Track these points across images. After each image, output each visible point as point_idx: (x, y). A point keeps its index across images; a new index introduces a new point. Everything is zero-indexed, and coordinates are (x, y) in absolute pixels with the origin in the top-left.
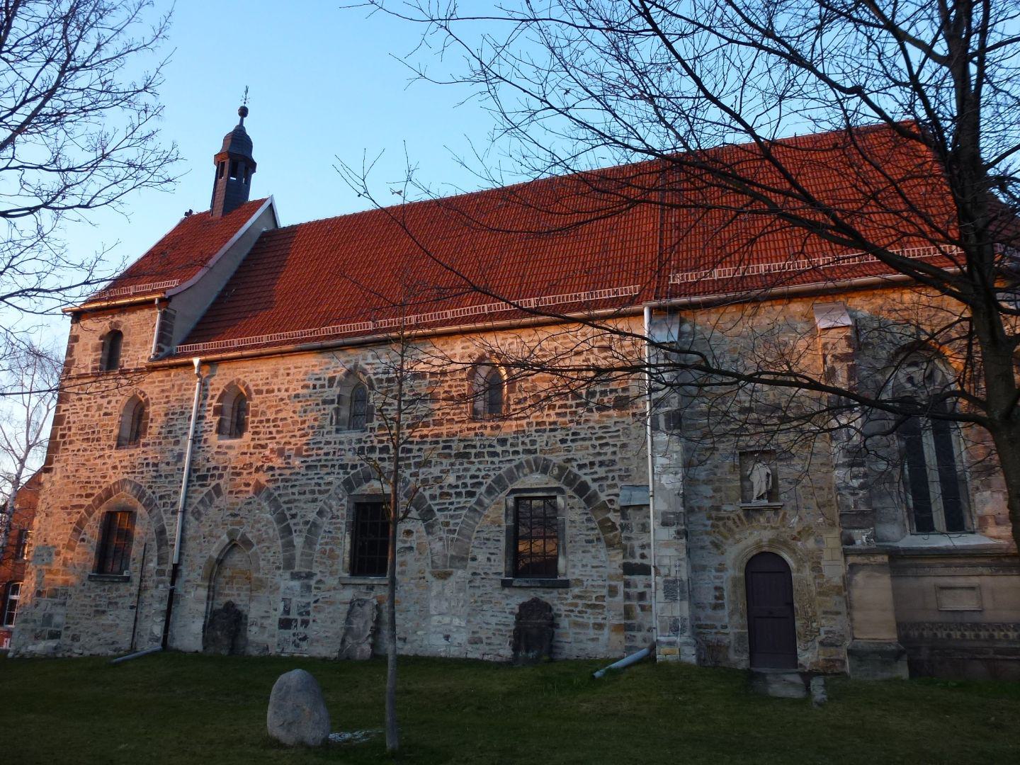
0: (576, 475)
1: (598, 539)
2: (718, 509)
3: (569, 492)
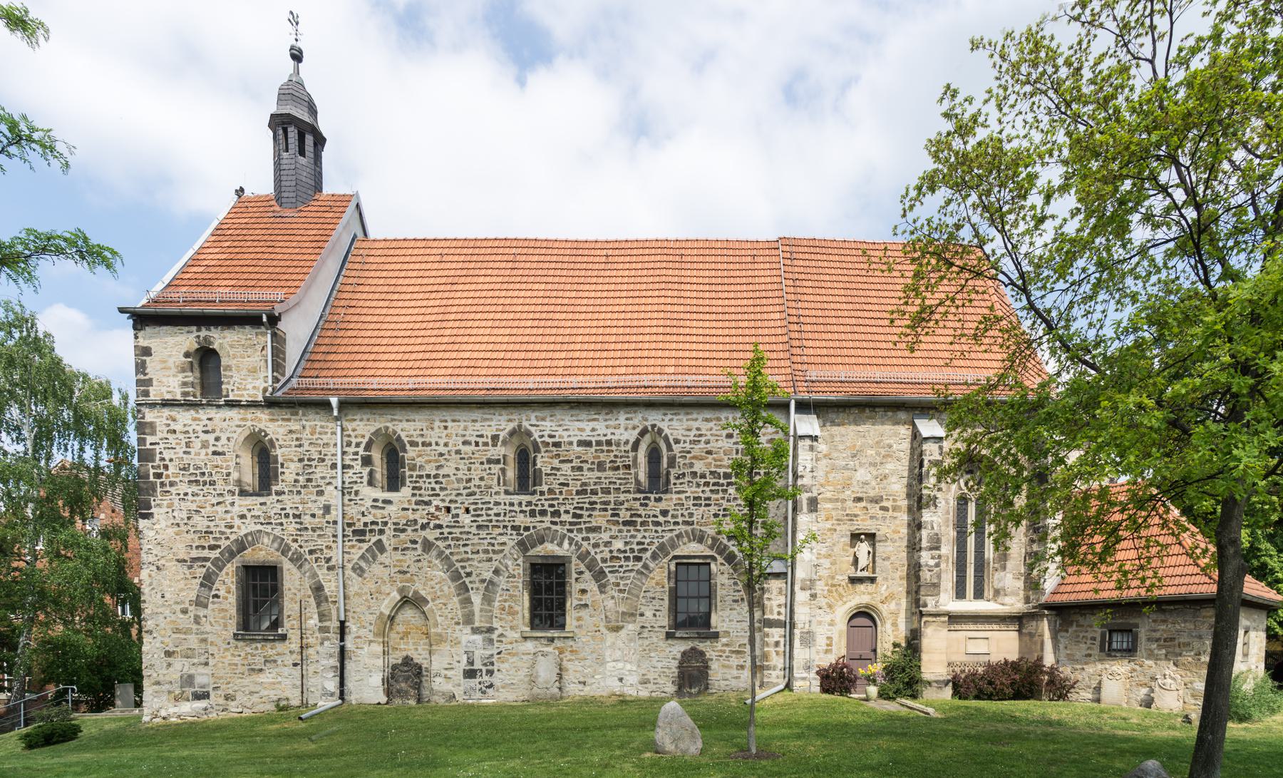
0: (725, 546)
1: (742, 599)
2: (833, 578)
3: (720, 560)
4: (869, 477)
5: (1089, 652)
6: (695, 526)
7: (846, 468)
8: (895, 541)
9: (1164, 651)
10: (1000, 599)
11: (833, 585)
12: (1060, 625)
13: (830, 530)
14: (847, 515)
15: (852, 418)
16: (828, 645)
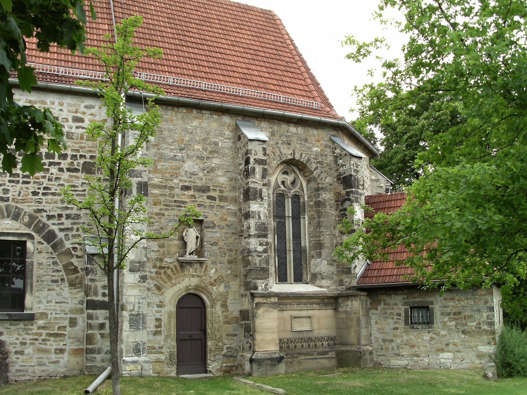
0: (44, 225)
1: (63, 280)
2: (161, 260)
3: (38, 238)
4: (196, 169)
5: (397, 326)
6: (10, 203)
7: (174, 158)
8: (223, 228)
9: (454, 323)
10: (318, 282)
11: (161, 268)
12: (371, 304)
13: (157, 214)
14: (175, 201)
15: (180, 116)
16: (157, 327)
